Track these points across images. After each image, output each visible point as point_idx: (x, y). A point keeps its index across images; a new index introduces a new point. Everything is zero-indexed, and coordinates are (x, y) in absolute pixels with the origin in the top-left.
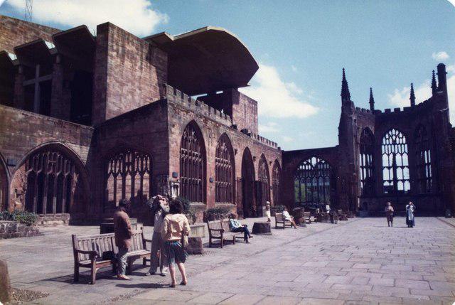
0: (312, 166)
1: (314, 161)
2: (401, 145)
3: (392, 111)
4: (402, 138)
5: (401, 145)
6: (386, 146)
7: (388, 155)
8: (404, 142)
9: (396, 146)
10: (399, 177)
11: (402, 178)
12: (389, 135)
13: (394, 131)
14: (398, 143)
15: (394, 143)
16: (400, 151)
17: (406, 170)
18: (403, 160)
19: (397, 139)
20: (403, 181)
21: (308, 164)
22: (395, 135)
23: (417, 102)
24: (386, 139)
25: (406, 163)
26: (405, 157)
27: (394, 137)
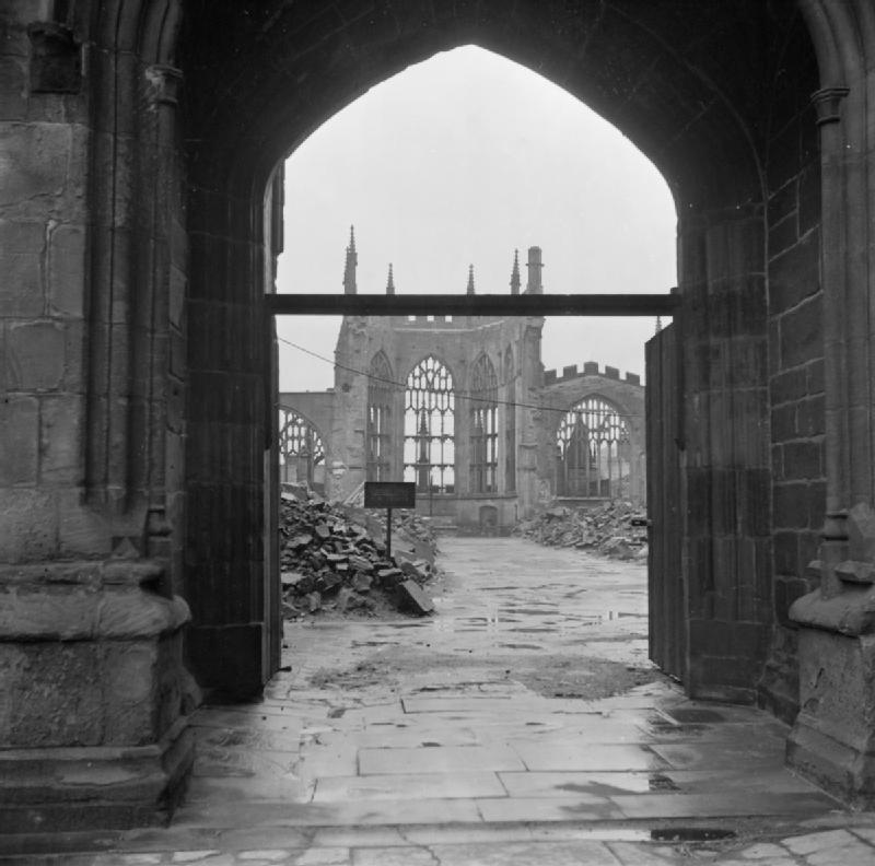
4: (446, 378)
6: (414, 393)
8: (449, 387)
10: (435, 459)
11: (439, 462)
13: (430, 361)
14: (436, 387)
15: (430, 389)
17: (450, 446)
18: (444, 424)
19: (437, 380)
20: (442, 467)
22: (433, 371)
24: (414, 377)
25: (450, 430)
26: (450, 419)
27: (430, 375)
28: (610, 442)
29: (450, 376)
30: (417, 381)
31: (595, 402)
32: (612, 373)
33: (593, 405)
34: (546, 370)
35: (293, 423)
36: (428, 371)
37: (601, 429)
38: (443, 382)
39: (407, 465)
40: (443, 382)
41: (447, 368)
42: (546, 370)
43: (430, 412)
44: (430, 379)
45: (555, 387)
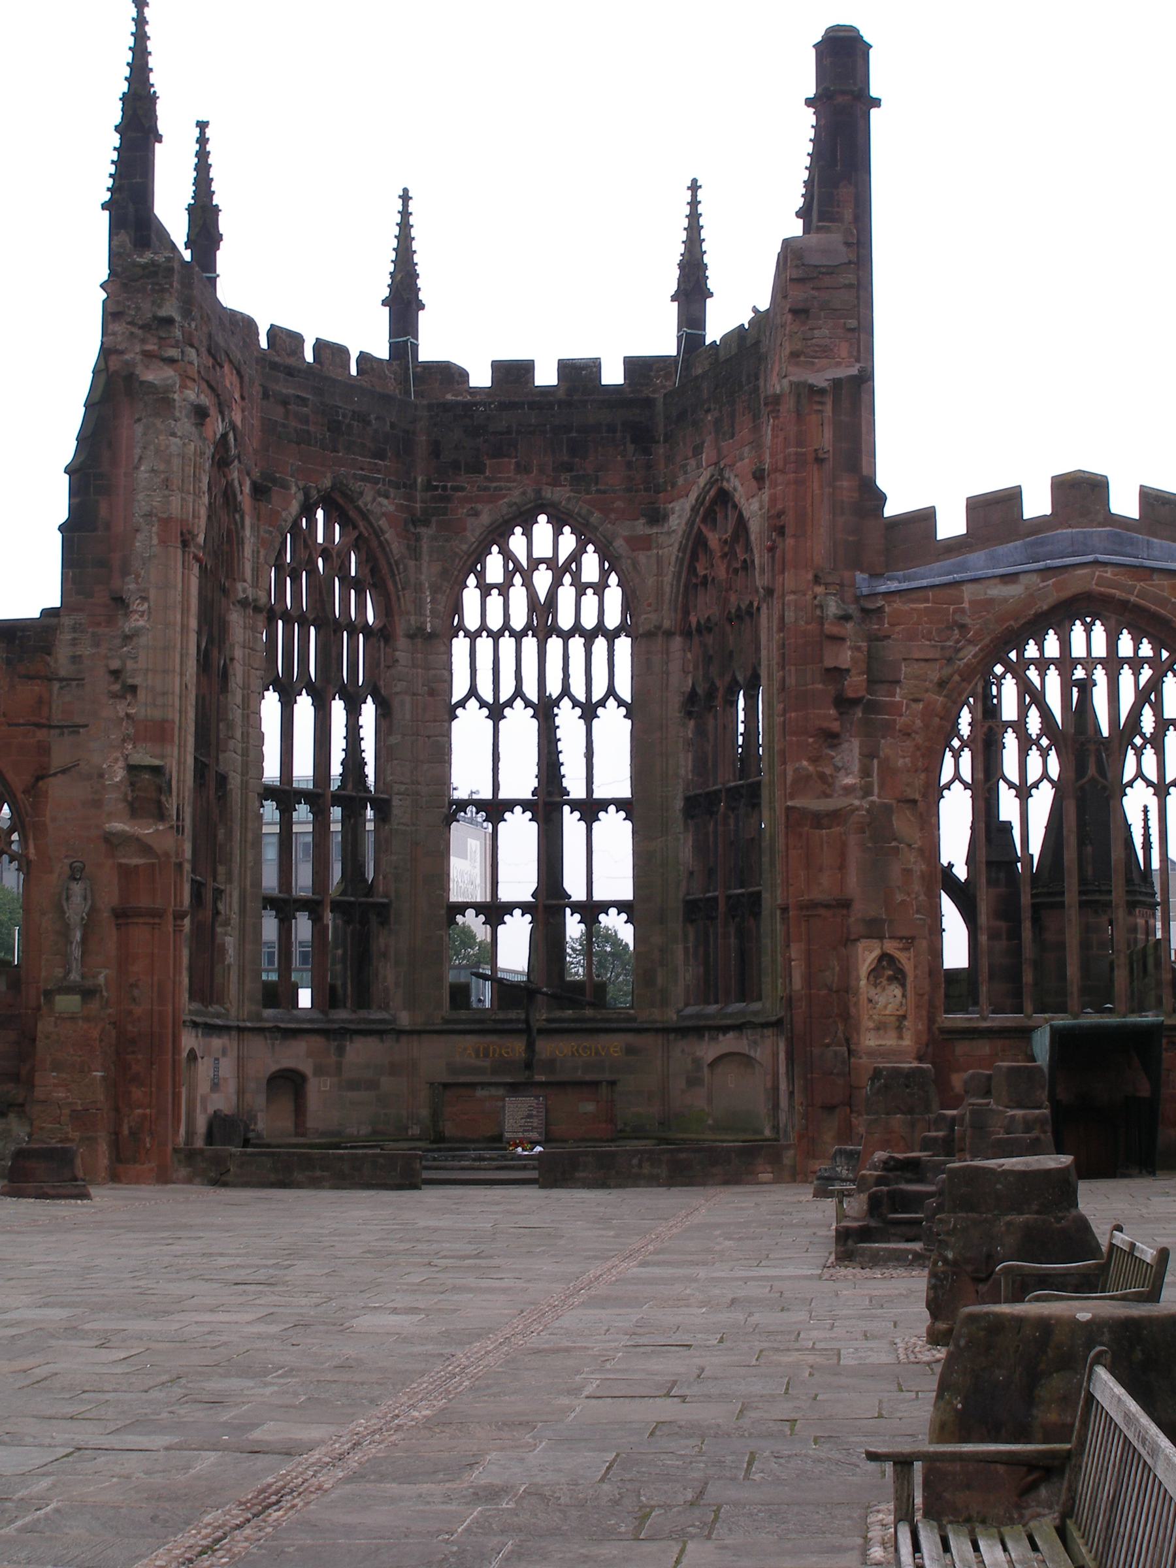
2: (589, 637)
3: (546, 376)
5: (589, 637)
6: (484, 644)
7: (496, 712)
9: (554, 645)
12: (507, 555)
13: (543, 528)
14: (565, 620)
16: (579, 692)
19: (566, 594)
22: (551, 563)
23: (715, 331)
24: (485, 590)
27: (542, 579)
29: (613, 579)
30: (495, 600)
31: (1099, 631)
34: (890, 511)
36: (535, 563)
38: (590, 601)
40: (590, 601)
41: (604, 555)
42: (890, 511)
44: (542, 590)
45: (931, 575)
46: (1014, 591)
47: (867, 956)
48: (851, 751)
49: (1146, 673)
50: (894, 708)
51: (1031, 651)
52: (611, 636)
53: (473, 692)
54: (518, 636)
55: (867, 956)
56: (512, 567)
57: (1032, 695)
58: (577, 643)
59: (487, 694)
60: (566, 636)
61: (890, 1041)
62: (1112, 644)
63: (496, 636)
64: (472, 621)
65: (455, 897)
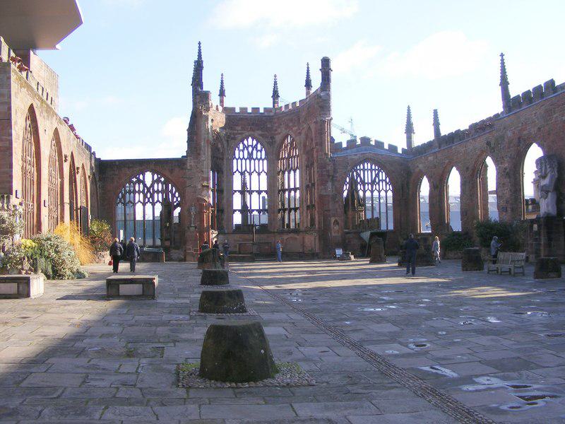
0: (145, 185)
1: (149, 178)
2: (259, 160)
3: (250, 111)
5: (259, 160)
6: (239, 161)
8: (263, 157)
9: (252, 161)
12: (244, 144)
13: (250, 139)
14: (254, 157)
15: (250, 157)
16: (257, 170)
18: (259, 182)
19: (255, 152)
21: (139, 181)
22: (252, 146)
23: (281, 104)
24: (239, 151)
25: (264, 187)
26: (264, 177)
27: (250, 149)
28: (379, 192)
30: (241, 153)
31: (369, 164)
32: (379, 144)
33: (367, 166)
34: (335, 142)
35: (158, 181)
36: (249, 146)
37: (373, 182)
38: (259, 153)
39: (235, 211)
40: (259, 153)
41: (262, 145)
42: (335, 142)
43: (250, 174)
46: (356, 157)
47: (333, 220)
48: (330, 184)
49: (377, 172)
50: (337, 177)
51: (358, 168)
52: (263, 160)
53: (237, 170)
54: (246, 160)
55: (333, 220)
56: (245, 147)
57: (359, 175)
58: (257, 161)
59: (240, 170)
60: (255, 160)
61: (337, 234)
62: (371, 167)
63: (241, 159)
64: (237, 157)
65: (234, 208)
